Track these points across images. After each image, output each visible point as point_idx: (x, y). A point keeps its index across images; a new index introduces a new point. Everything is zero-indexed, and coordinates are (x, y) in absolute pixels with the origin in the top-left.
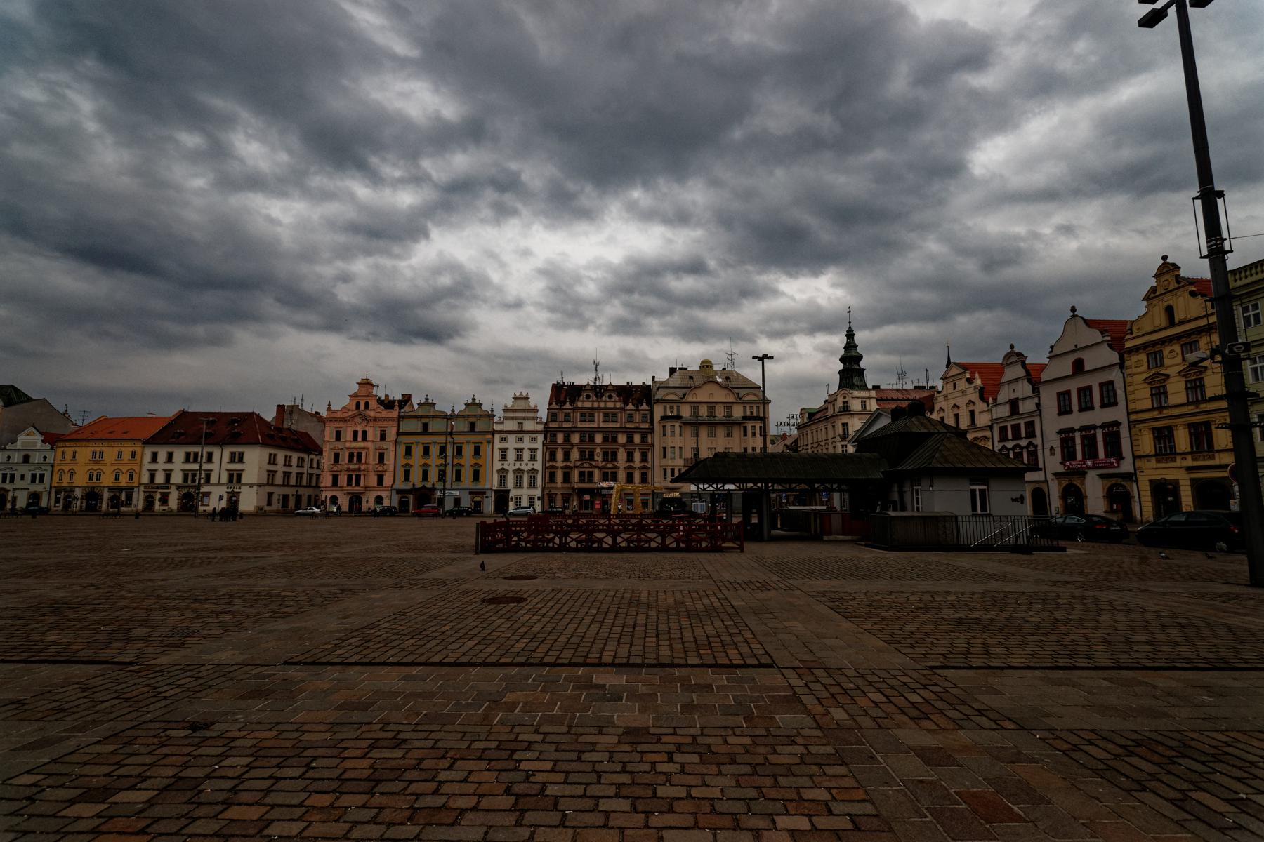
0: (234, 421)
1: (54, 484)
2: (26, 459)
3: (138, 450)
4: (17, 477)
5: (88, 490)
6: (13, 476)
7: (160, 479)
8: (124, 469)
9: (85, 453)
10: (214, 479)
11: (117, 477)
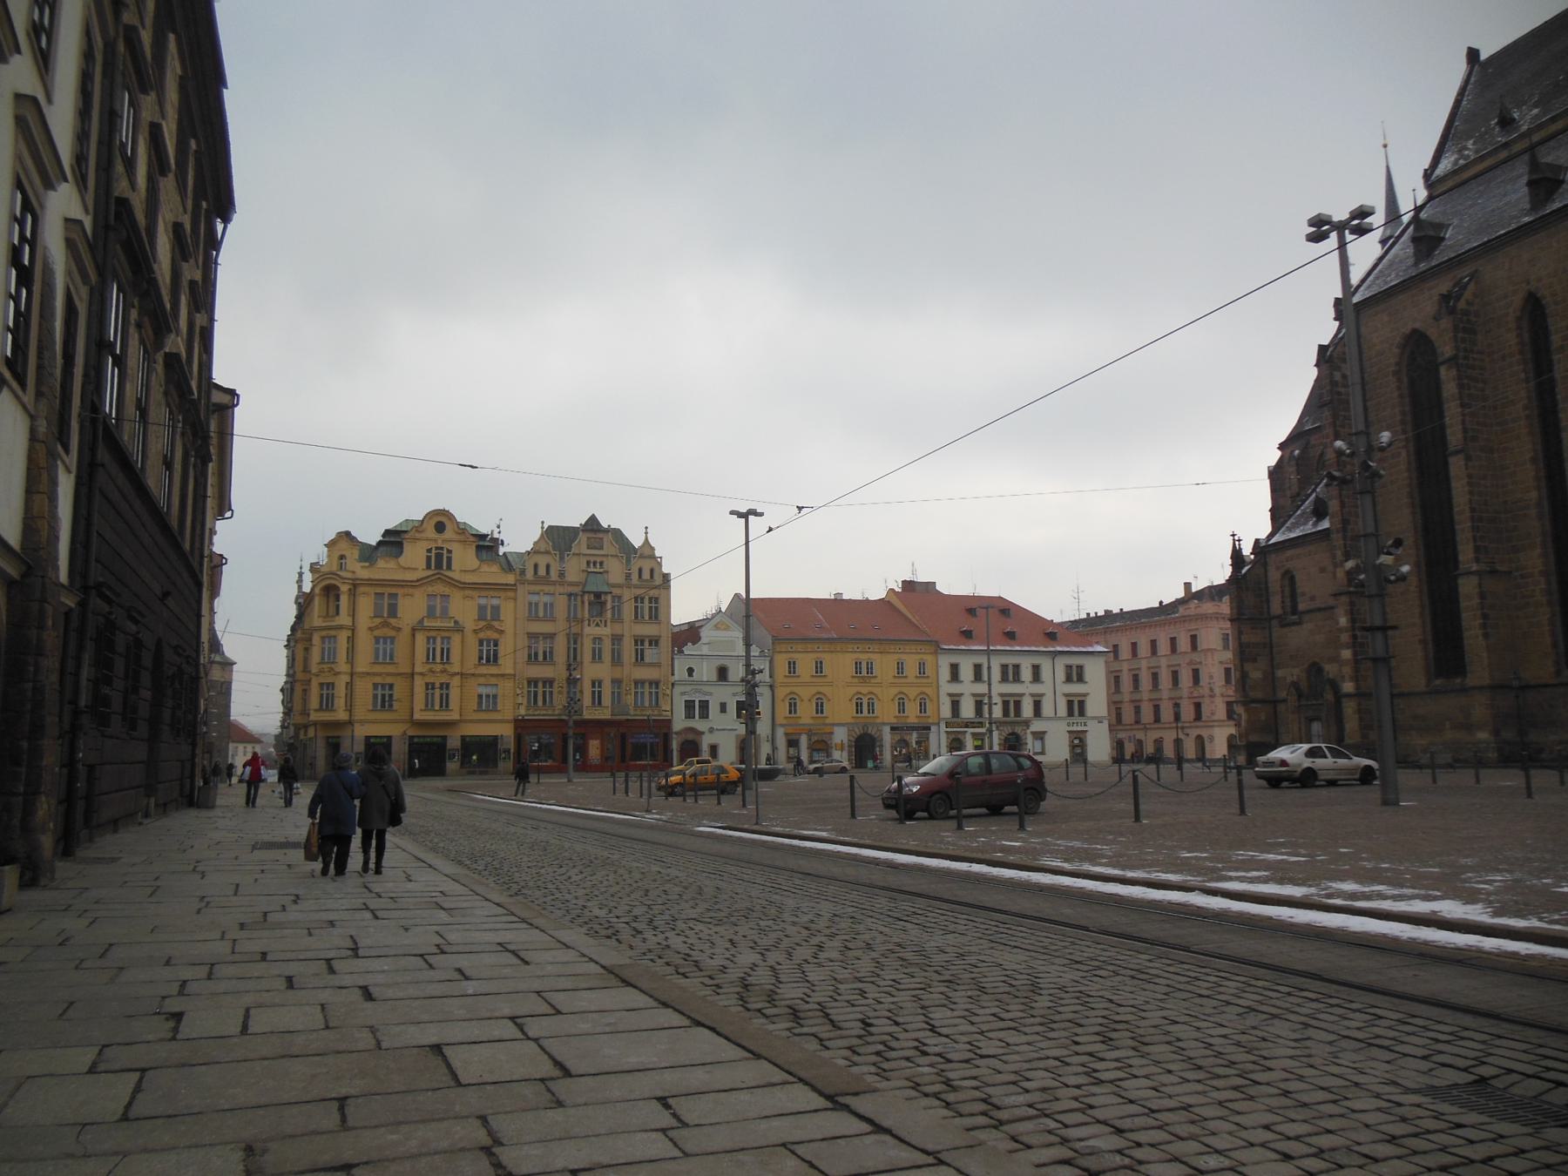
0: (971, 611)
1: (780, 720)
2: (722, 673)
3: (929, 659)
4: (714, 709)
5: (858, 732)
6: (704, 705)
7: (968, 711)
8: (913, 692)
9: (840, 664)
10: (1047, 709)
11: (902, 708)
